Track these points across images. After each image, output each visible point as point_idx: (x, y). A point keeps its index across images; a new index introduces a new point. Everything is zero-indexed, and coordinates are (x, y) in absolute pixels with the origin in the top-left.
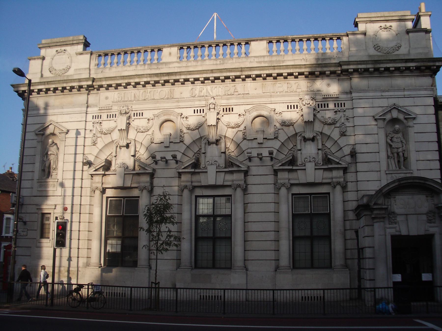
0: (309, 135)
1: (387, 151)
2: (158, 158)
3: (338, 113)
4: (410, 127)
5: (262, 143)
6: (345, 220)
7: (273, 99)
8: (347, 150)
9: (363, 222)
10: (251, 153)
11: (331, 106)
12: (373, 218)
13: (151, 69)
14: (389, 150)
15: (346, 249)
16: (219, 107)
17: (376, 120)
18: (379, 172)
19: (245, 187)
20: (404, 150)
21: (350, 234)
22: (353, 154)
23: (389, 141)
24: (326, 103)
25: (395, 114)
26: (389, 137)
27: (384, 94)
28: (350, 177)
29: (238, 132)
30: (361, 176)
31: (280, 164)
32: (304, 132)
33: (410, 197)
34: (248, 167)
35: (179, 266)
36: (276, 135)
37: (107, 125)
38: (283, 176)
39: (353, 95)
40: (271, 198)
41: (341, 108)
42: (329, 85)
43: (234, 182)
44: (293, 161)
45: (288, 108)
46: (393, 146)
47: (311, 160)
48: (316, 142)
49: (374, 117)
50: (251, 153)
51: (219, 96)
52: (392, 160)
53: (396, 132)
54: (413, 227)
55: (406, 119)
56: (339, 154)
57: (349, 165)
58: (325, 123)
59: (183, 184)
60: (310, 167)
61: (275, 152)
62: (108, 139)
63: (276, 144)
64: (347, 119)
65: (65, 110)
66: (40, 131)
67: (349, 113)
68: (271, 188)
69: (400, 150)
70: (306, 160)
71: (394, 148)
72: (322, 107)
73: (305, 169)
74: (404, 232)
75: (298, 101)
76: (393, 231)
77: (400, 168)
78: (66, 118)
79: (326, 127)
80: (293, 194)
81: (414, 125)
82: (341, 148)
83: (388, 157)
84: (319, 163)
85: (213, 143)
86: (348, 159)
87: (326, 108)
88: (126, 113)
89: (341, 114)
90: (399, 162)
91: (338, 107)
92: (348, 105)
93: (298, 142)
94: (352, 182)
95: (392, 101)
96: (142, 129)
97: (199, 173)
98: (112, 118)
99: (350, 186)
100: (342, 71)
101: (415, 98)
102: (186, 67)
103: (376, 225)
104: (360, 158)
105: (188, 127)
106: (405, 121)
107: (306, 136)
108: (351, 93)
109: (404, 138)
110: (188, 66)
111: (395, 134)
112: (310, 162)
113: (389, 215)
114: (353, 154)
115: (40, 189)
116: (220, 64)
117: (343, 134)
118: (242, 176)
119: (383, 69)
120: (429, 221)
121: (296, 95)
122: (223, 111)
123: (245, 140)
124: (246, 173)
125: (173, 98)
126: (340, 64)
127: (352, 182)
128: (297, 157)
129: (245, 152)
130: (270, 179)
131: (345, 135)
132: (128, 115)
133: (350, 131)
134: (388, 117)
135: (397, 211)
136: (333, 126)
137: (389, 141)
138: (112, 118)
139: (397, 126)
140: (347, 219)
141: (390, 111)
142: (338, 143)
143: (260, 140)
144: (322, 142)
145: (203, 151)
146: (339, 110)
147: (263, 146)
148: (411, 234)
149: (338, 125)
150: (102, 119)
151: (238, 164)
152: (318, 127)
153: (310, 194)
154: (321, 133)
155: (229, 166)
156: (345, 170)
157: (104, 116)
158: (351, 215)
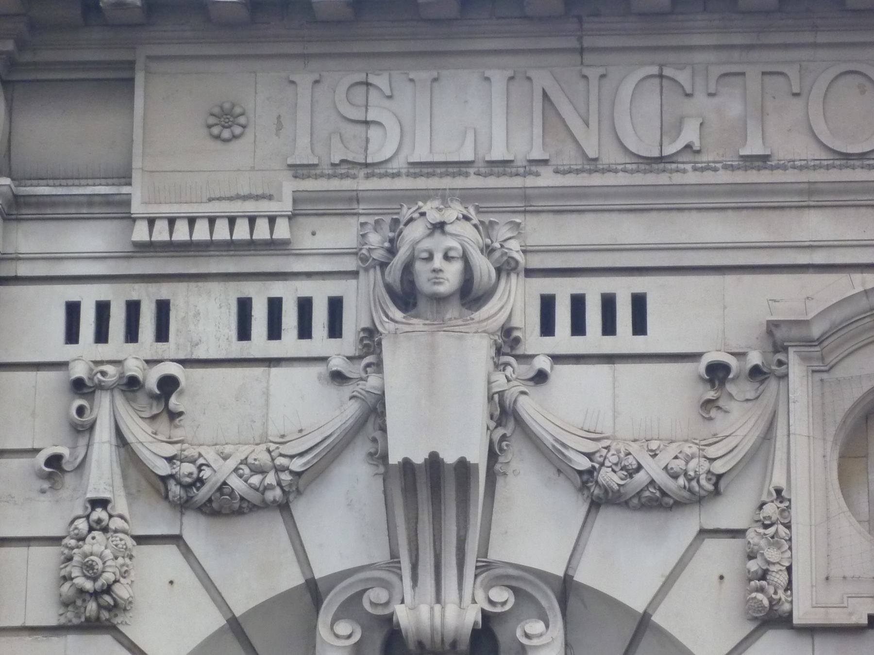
62: (253, 569)
88: (470, 295)
96: (653, 470)
98: (290, 343)
132: (493, 313)
138: (290, 343)
150: (172, 348)
157: (205, 317)
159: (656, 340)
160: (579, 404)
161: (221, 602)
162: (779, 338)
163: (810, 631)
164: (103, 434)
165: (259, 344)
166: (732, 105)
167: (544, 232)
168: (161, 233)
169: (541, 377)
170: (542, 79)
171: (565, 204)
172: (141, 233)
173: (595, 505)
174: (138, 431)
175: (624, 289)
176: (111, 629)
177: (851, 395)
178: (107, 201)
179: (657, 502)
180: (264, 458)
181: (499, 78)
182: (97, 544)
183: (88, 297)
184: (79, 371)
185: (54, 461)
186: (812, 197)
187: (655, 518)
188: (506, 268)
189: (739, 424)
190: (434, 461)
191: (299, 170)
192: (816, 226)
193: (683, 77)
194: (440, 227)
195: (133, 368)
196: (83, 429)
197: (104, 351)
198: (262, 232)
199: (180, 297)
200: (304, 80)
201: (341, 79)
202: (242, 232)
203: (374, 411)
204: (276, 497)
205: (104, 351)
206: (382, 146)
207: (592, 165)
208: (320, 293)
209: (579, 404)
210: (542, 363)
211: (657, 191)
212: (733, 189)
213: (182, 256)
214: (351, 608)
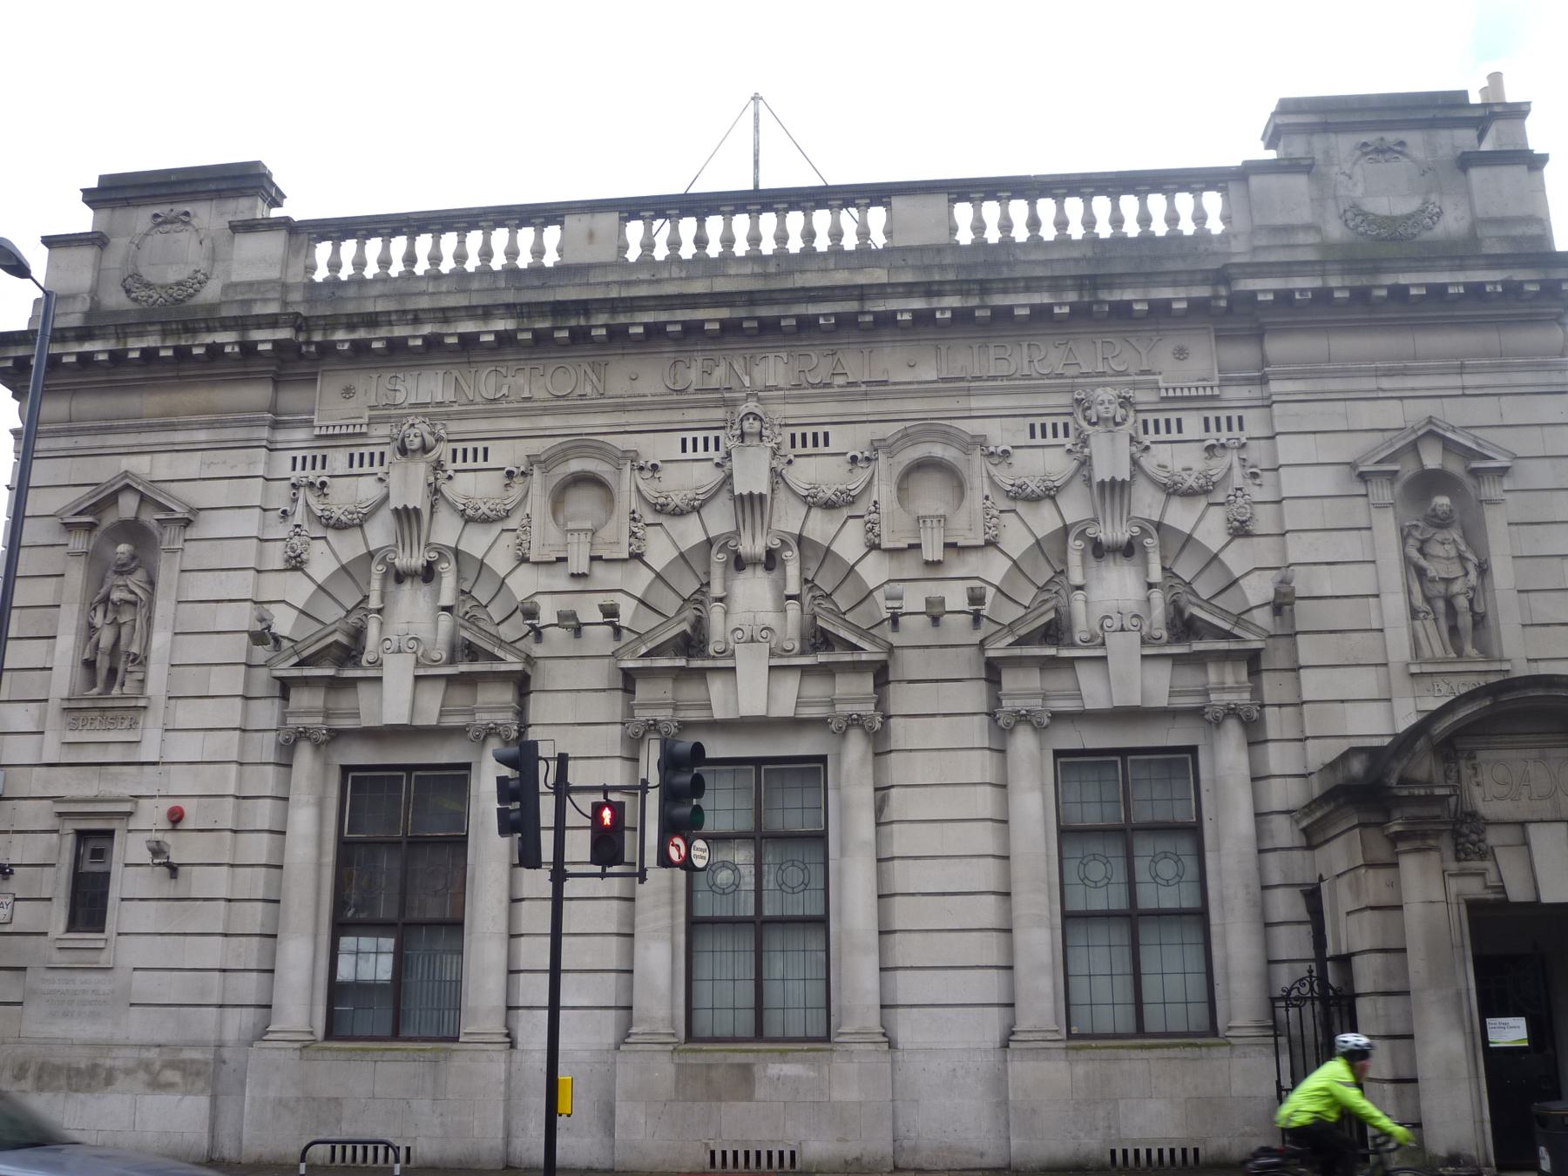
0: (1113, 532)
1: (1410, 592)
2: (547, 615)
3: (1218, 452)
4: (1490, 502)
5: (939, 562)
6: (1260, 851)
7: (975, 403)
8: (1258, 590)
9: (1338, 854)
10: (900, 598)
11: (1193, 425)
12: (1395, 839)
13: (518, 289)
14: (1416, 588)
16: (777, 429)
18: (1381, 670)
19: (878, 726)
20: (1473, 589)
21: (1285, 905)
23: (1414, 554)
24: (1173, 416)
25: (1432, 459)
26: (1411, 541)
27: (1386, 383)
28: (1273, 688)
29: (851, 521)
30: (1313, 684)
31: (1010, 640)
32: (1095, 520)
33: (1534, 753)
34: (891, 649)
35: (625, 1036)
36: (993, 532)
38: (1021, 687)
39: (1275, 386)
40: (980, 766)
41: (1230, 435)
42: (1181, 354)
43: (838, 707)
44: (1055, 631)
45: (1033, 436)
46: (1432, 572)
47: (1127, 624)
48: (1137, 558)
49: (1352, 465)
50: (900, 598)
51: (776, 388)
52: (1429, 623)
53: (1441, 522)
55: (1474, 473)
56: (1227, 602)
57: (1270, 641)
58: (1172, 491)
59: (642, 715)
60: (1123, 649)
61: (990, 593)
62: (349, 547)
63: (995, 569)
64: (1254, 475)
66: (80, 513)
67: (1258, 454)
68: (976, 731)
69: (1457, 587)
70: (1108, 622)
71: (1433, 580)
72: (1157, 431)
73: (1104, 658)
74: (1518, 892)
75: (1069, 410)
76: (1474, 888)
77: (1460, 652)
78: (189, 465)
79: (1176, 505)
80: (1058, 754)
81: (1507, 496)
82: (1236, 581)
83: (1414, 613)
84: (1157, 634)
85: (754, 563)
86: (1263, 618)
87: (1174, 435)
88: (425, 449)
89: (1232, 457)
90: (1454, 630)
91: (1219, 429)
92: (1255, 424)
93: (1074, 558)
94: (1280, 706)
95: (1417, 412)
96: (484, 509)
97: (702, 673)
98: (366, 469)
99: (1276, 723)
100: (1233, 299)
101: (1503, 398)
102: (650, 282)
103: (1411, 865)
104: (1305, 615)
105: (661, 500)
106: (1469, 482)
107: (1102, 536)
108: (1263, 380)
109: (1468, 544)
110: (658, 281)
111: (1432, 530)
112: (1122, 630)
114: (1281, 604)
115: (72, 737)
116: (777, 274)
117: (1240, 531)
118: (866, 684)
119: (1384, 293)
121: (1065, 385)
122: (793, 446)
123: (874, 553)
124: (881, 674)
126: (1222, 276)
127: (1280, 706)
128: (1069, 615)
129: (879, 596)
130: (973, 696)
131: (1248, 534)
132: (432, 455)
133: (1264, 520)
134: (1407, 469)
135: (1488, 809)
136: (1202, 502)
137: (1414, 554)
139: (1442, 501)
140: (1268, 845)
141: (1414, 447)
142: (1222, 564)
143: (933, 552)
144: (1163, 558)
145: (716, 589)
146: (1223, 441)
150: (326, 472)
151: (854, 639)
152: (1147, 503)
153: (1123, 752)
154: (1159, 526)
155: (815, 649)
158: (1284, 832)
159: (491, 464)
160: (805, 473)
161: (677, 547)
162: (532, 460)
163: (886, 550)
164: (301, 502)
165: (356, 469)
166: (521, 380)
167: (454, 427)
168: (324, 432)
169: (450, 478)
170: (456, 373)
171: (462, 416)
172: (317, 432)
173: (467, 522)
174: (312, 501)
175: (480, 445)
176: (301, 569)
177: (898, 470)
178: (307, 421)
179: (486, 520)
180: (352, 508)
181: (441, 373)
182: (296, 540)
183: (299, 454)
184: (293, 480)
185: (284, 512)
186: (546, 411)
187: (486, 526)
188: (439, 440)
189: (516, 491)
190: (405, 507)
191: (372, 408)
192: (547, 421)
193: (503, 371)
194: (412, 425)
195: (311, 479)
196: (295, 501)
197: (304, 473)
198: (357, 430)
199: (329, 453)
200: (375, 376)
201: (387, 375)
202: (351, 430)
204: (356, 523)
205: (304, 473)
206: (400, 398)
207: (472, 402)
208: (377, 450)
210: (450, 473)
211: (493, 411)
212: (486, 411)
213: (330, 439)
214: (383, 560)
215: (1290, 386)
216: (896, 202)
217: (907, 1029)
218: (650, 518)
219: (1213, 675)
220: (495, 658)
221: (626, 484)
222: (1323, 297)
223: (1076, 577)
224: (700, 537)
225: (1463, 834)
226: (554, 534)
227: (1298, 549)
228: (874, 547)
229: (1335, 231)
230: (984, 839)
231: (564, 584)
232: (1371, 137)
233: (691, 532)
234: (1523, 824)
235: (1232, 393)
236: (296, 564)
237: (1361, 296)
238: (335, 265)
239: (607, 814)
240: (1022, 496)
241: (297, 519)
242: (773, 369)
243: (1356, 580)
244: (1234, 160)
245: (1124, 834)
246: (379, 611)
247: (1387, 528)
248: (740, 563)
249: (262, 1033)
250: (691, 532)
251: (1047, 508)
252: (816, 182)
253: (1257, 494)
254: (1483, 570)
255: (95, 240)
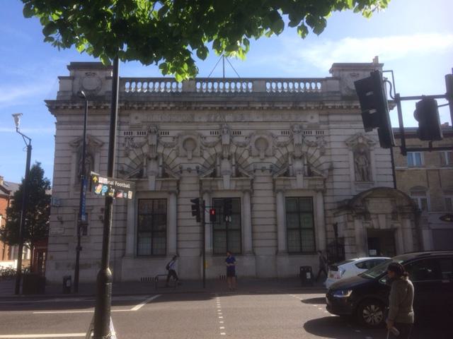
0: (298, 153)
8: (325, 166)
9: (340, 219)
11: (314, 133)
15: (327, 239)
17: (347, 144)
21: (330, 228)
22: (331, 169)
25: (361, 141)
27: (353, 125)
30: (336, 185)
37: (138, 140)
42: (312, 118)
46: (359, 164)
54: (382, 223)
62: (139, 152)
65: (99, 126)
68: (270, 193)
74: (376, 226)
76: (368, 225)
83: (355, 172)
90: (363, 175)
92: (326, 133)
93: (290, 159)
97: (216, 181)
99: (328, 193)
104: (336, 172)
108: (328, 124)
113: (365, 215)
114: (331, 169)
117: (322, 154)
120: (393, 219)
125: (194, 122)
133: (328, 153)
134: (356, 142)
135: (371, 211)
145: (218, 163)
147: (264, 161)
148: (382, 228)
149: (319, 147)
156: (325, 181)
157: (135, 133)
203: (148, 141)
209: (164, 140)
215: (334, 125)
216: (254, 82)
217: (258, 251)
218: (204, 148)
219: (317, 182)
220: (173, 177)
221: (199, 141)
222: (341, 107)
223: (290, 162)
224: (214, 153)
225: (365, 215)
226: (184, 151)
227: (334, 159)
228: (250, 155)
229: (344, 92)
230: (272, 214)
231: (186, 161)
232: (352, 72)
233: (213, 151)
234: (377, 214)
235: (322, 126)
236: (127, 155)
237: (349, 107)
238: (130, 88)
239: (213, 212)
240: (279, 145)
241: (127, 145)
242: (229, 117)
243: (344, 165)
244: (324, 77)
245: (299, 212)
246: (146, 166)
247: (351, 154)
248: (222, 158)
249: (124, 255)
250: (213, 151)
251: (285, 149)
252: (237, 77)
253: (326, 147)
254: (369, 163)
255: (72, 78)
